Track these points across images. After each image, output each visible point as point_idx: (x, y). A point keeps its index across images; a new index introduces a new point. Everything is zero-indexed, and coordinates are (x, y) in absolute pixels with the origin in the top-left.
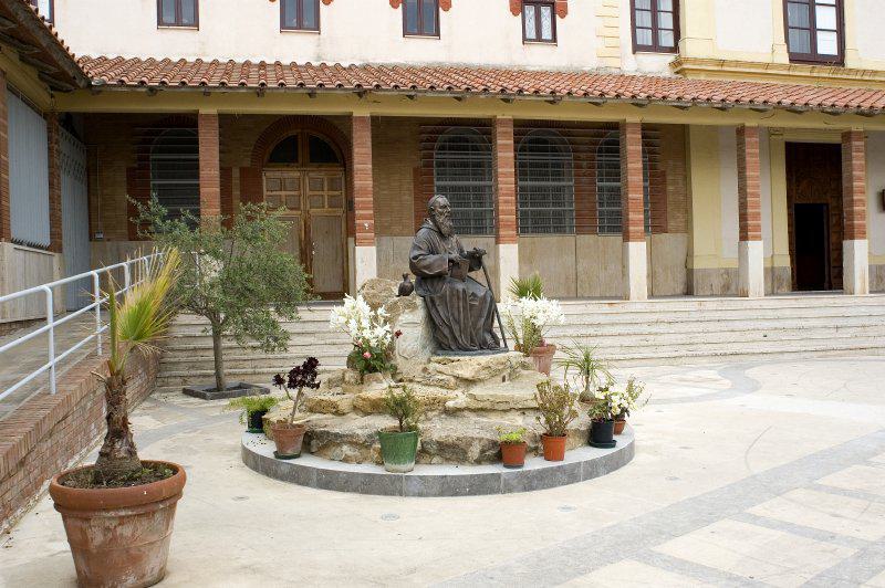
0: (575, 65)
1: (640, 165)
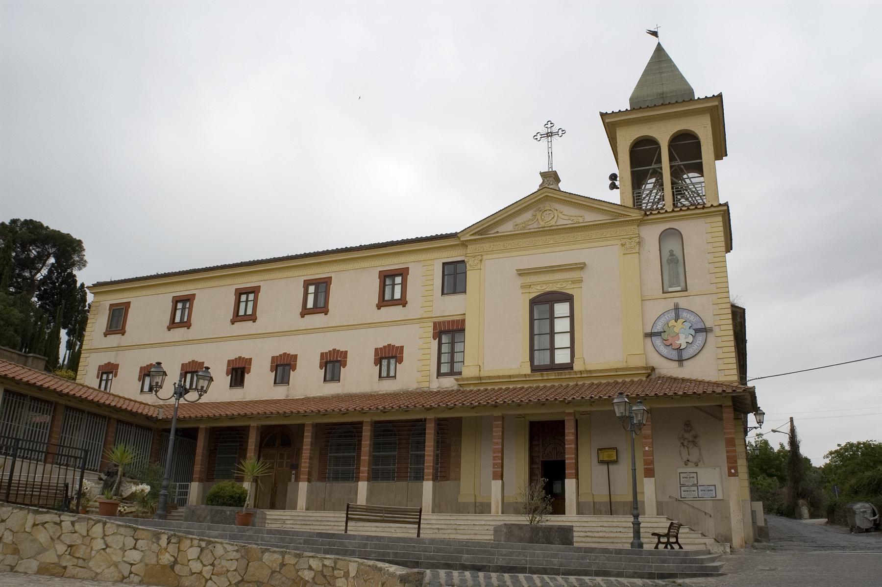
0: (405, 388)
1: (368, 442)
